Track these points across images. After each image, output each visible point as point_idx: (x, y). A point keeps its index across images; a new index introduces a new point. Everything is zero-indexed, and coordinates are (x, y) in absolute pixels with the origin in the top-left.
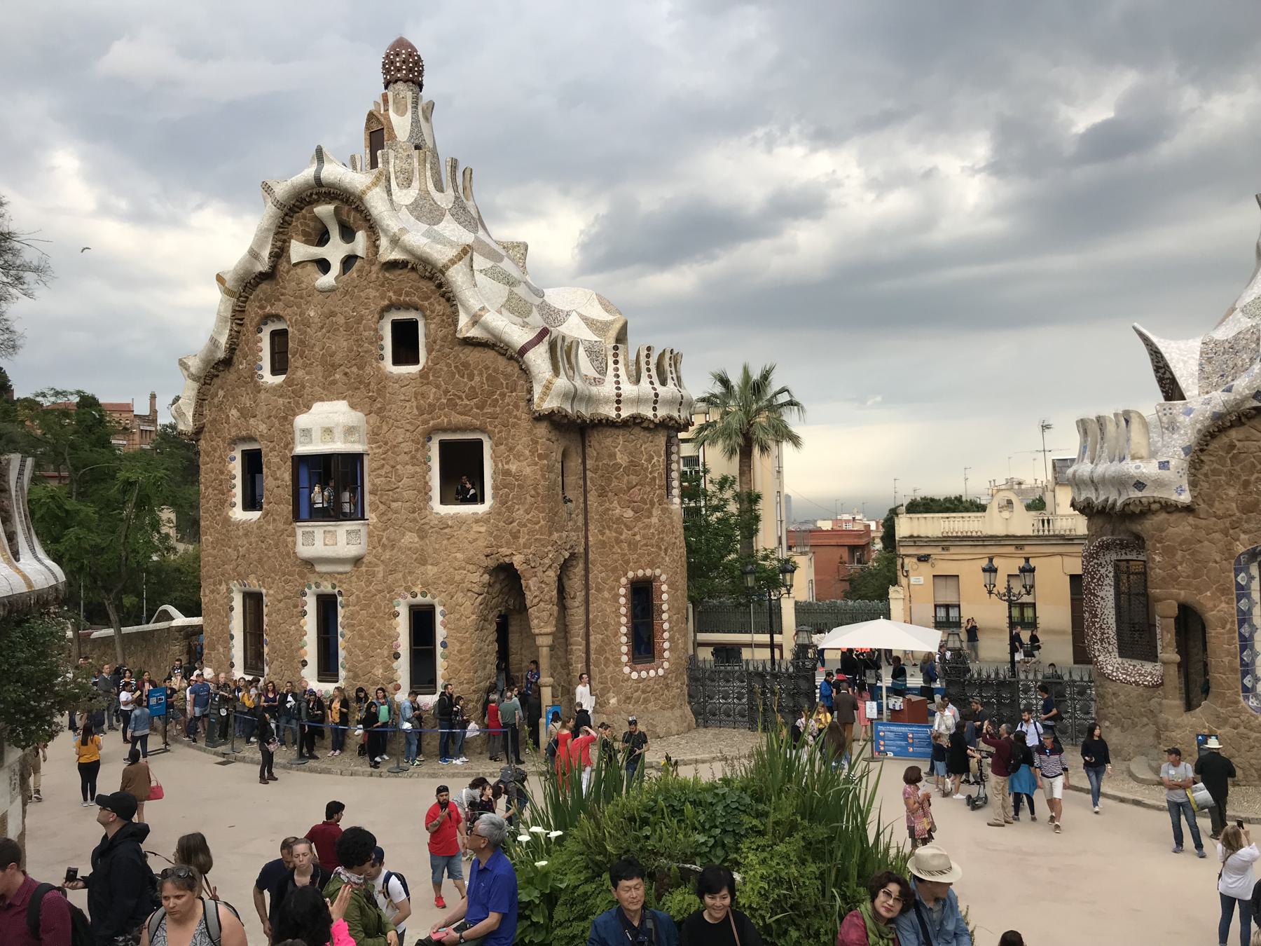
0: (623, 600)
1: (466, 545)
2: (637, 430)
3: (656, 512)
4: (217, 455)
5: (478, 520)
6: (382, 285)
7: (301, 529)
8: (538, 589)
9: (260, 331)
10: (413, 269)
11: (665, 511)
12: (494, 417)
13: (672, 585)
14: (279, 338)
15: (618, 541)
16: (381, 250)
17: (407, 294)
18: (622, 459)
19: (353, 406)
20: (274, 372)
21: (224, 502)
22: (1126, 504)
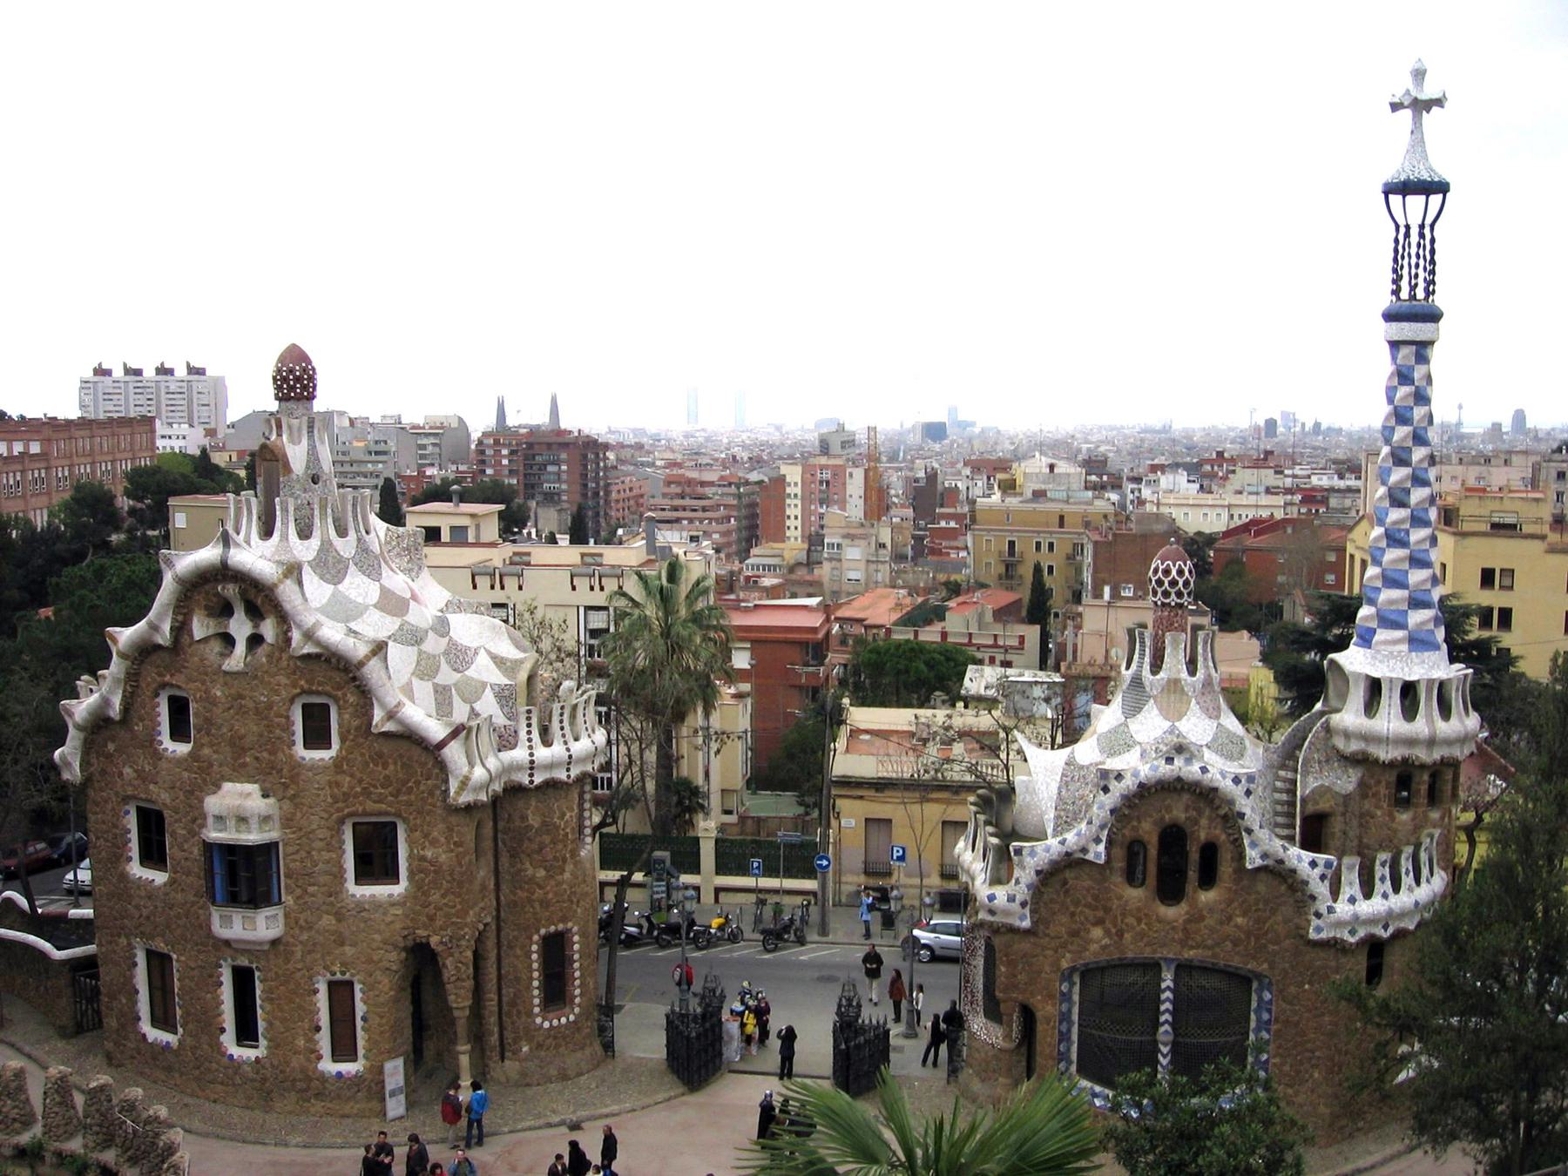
0: (535, 956)
1: (383, 927)
2: (550, 791)
3: (569, 867)
4: (109, 806)
5: (393, 903)
6: (294, 673)
7: (216, 915)
8: (455, 968)
9: (157, 695)
11: (575, 864)
13: (583, 934)
15: (530, 901)
16: (294, 644)
17: (319, 684)
18: (534, 820)
21: (119, 857)
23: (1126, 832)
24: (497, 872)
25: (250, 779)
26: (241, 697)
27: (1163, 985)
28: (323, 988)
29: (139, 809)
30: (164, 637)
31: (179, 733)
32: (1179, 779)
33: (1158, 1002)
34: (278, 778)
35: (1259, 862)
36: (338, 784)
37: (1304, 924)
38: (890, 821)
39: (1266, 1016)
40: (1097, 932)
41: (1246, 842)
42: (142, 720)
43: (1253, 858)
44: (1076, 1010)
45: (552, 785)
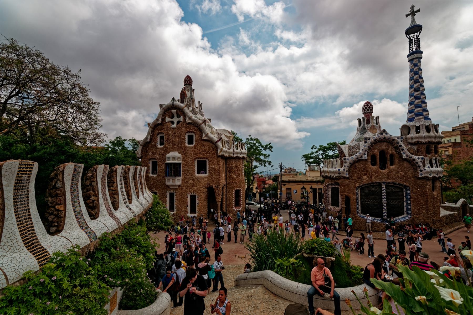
2: (237, 159)
3: (240, 176)
8: (218, 192)
10: (194, 125)
12: (209, 156)
14: (162, 138)
15: (233, 182)
18: (234, 165)
19: (179, 153)
20: (160, 145)
22: (336, 177)
23: (371, 153)
24: (226, 176)
25: (176, 151)
26: (175, 133)
27: (383, 189)
28: (189, 197)
29: (152, 162)
30: (160, 121)
31: (161, 144)
32: (385, 138)
33: (382, 193)
34: (183, 150)
35: (406, 157)
36: (194, 151)
37: (417, 174)
38: (290, 189)
39: (409, 197)
40: (365, 177)
41: (402, 152)
42: (154, 141)
43: (404, 156)
44: (359, 197)
45: (238, 158)
